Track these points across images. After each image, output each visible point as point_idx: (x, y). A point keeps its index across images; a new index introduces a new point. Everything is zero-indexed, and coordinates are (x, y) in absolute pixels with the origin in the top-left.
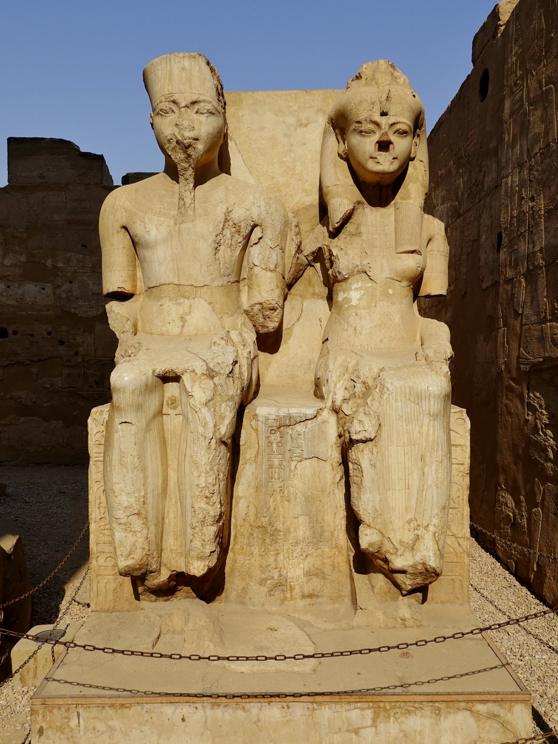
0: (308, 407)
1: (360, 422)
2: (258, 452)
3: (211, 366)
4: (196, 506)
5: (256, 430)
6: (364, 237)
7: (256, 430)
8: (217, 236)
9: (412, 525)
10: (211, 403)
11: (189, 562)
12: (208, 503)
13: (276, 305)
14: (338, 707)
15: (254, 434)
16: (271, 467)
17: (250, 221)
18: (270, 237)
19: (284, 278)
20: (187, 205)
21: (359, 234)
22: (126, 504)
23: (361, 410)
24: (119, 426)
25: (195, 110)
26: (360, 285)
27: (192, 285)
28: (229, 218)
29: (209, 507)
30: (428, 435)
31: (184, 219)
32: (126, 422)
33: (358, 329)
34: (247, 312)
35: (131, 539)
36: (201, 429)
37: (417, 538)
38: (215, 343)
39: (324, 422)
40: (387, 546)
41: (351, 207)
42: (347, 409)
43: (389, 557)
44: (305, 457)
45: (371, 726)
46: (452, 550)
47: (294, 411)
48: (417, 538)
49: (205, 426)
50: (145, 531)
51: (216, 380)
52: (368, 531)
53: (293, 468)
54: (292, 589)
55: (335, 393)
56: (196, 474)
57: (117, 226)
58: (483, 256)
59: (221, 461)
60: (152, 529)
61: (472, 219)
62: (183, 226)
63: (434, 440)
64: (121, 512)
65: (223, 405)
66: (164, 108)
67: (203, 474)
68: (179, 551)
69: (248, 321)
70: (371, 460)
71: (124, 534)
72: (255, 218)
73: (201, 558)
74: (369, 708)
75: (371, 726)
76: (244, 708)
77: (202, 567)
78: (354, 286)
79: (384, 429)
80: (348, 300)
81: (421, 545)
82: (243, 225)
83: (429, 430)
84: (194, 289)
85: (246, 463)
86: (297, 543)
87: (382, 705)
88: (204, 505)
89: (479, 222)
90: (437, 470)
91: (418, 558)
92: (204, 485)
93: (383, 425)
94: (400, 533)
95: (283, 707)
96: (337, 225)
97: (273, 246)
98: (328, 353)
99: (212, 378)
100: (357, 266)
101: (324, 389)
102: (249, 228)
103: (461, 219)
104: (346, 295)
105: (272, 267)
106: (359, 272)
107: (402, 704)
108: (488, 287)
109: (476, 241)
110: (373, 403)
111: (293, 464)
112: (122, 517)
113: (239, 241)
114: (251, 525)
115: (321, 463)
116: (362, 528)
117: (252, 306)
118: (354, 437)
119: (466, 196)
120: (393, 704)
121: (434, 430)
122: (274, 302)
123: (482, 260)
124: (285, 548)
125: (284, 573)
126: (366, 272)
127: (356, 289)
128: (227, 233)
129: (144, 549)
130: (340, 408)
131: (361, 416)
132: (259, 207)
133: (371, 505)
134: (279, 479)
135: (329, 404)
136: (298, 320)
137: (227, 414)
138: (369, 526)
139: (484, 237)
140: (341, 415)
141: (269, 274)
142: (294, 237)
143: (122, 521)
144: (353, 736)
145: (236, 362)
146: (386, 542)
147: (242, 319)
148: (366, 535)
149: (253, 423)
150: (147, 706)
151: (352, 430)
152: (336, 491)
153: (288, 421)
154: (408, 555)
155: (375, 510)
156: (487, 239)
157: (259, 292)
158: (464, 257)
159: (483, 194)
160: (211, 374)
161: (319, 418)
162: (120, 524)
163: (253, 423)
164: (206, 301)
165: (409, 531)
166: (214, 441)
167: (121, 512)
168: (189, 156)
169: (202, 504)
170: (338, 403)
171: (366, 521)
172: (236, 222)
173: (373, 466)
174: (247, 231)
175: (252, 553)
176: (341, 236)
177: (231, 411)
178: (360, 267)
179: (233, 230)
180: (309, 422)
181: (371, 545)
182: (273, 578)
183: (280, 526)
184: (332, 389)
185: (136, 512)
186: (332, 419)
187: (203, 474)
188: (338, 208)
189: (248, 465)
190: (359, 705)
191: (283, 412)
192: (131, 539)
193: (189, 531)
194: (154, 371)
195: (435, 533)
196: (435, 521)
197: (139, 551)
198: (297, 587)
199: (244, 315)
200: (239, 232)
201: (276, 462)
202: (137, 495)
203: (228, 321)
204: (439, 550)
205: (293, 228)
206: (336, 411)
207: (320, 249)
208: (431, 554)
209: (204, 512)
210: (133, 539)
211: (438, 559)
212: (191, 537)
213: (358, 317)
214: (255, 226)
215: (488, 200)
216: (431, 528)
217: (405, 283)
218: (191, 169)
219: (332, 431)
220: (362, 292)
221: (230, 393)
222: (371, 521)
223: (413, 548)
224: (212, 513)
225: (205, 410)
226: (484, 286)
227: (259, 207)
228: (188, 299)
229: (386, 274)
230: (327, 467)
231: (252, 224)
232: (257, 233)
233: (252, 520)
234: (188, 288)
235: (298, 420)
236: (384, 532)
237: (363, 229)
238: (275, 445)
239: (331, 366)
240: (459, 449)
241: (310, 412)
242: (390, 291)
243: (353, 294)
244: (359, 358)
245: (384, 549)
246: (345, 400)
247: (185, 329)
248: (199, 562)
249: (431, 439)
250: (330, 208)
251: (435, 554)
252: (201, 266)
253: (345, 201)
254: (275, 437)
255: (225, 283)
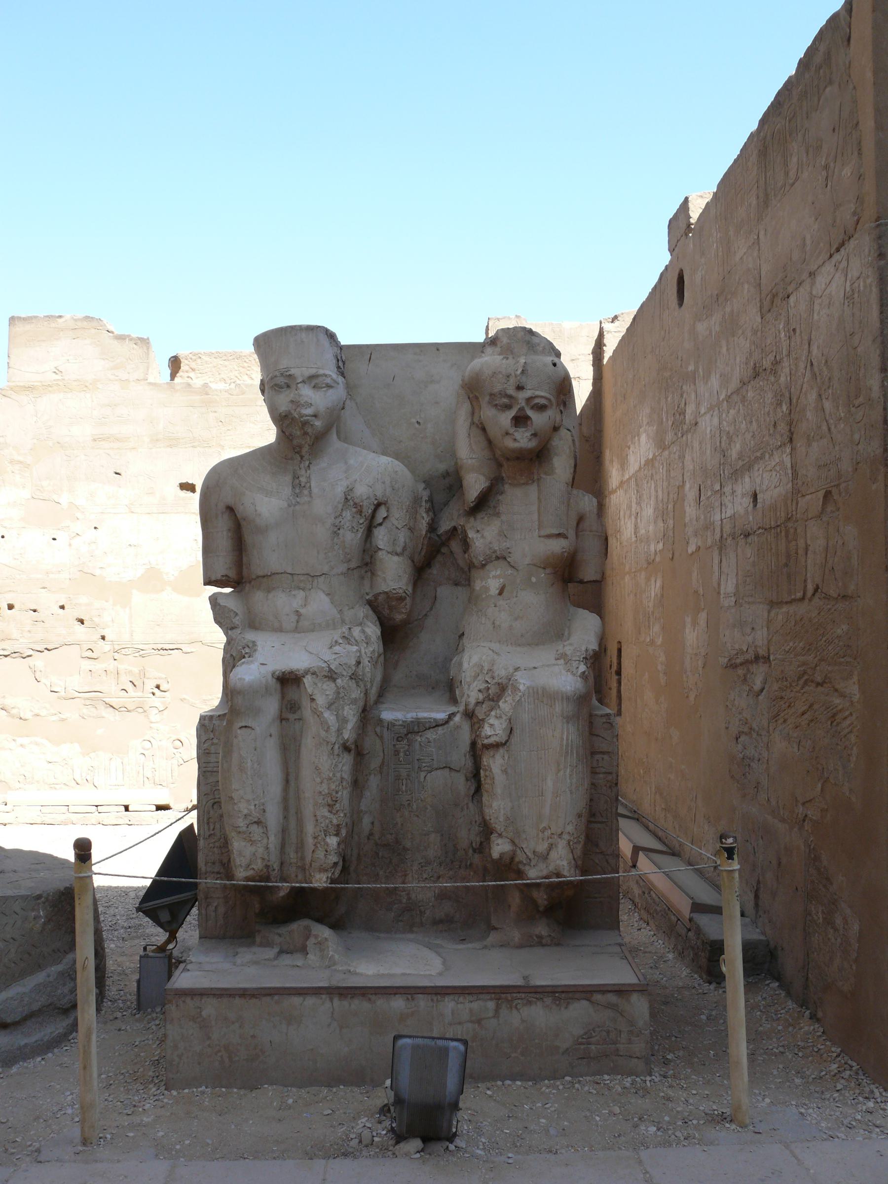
0: (438, 712)
1: (491, 725)
2: (383, 762)
3: (333, 667)
4: (318, 813)
5: (381, 738)
6: (504, 518)
7: (381, 738)
8: (336, 518)
9: (546, 833)
10: (333, 707)
11: (310, 875)
12: (329, 811)
13: (404, 595)
14: (461, 999)
15: (378, 741)
16: (398, 778)
17: (373, 500)
18: (398, 516)
19: (413, 561)
20: (303, 485)
21: (498, 515)
22: (246, 812)
23: (493, 713)
24: (239, 731)
25: (313, 384)
26: (498, 573)
27: (307, 574)
28: (349, 497)
29: (332, 816)
30: (562, 739)
31: (298, 500)
32: (246, 727)
33: (497, 623)
34: (370, 603)
35: (249, 850)
36: (323, 734)
37: (551, 847)
38: (336, 642)
39: (458, 727)
40: (520, 857)
41: (487, 484)
42: (480, 713)
43: (521, 866)
44: (435, 766)
45: (494, 1017)
46: (599, 869)
47: (423, 715)
48: (551, 847)
49: (327, 730)
50: (265, 841)
51: (339, 681)
52: (500, 841)
53: (422, 780)
54: (422, 913)
55: (468, 696)
56: (318, 780)
57: (221, 506)
58: (687, 509)
59: (344, 768)
60: (272, 838)
61: (676, 456)
62: (297, 507)
63: (567, 745)
64: (241, 820)
65: (346, 708)
66: (278, 382)
67: (325, 781)
68: (299, 864)
69: (371, 612)
70: (502, 766)
71: (243, 844)
72: (379, 494)
73: (322, 870)
74: (491, 999)
75: (494, 1017)
76: (370, 999)
77: (324, 879)
78: (493, 573)
79: (517, 732)
80: (487, 589)
81: (553, 855)
82: (365, 503)
83: (563, 733)
84: (310, 579)
85: (370, 774)
86: (428, 863)
87: (503, 996)
88: (327, 814)
89: (683, 463)
90: (570, 775)
91: (551, 868)
92: (326, 791)
93: (514, 729)
94: (534, 844)
95: (408, 999)
96: (472, 505)
97: (400, 527)
98: (463, 650)
99: (334, 680)
100: (495, 552)
101: (457, 693)
102: (373, 507)
103: (666, 453)
104: (484, 583)
105: (399, 550)
106: (498, 558)
107: (523, 995)
108: (692, 553)
109: (681, 487)
110: (506, 705)
111: (423, 774)
112: (242, 825)
113: (361, 522)
114: (377, 844)
115: (453, 774)
116: (493, 837)
117: (376, 596)
118: (486, 741)
119: (670, 423)
120: (515, 995)
121: (568, 733)
122: (401, 591)
123: (687, 515)
124: (415, 868)
125: (413, 896)
126: (505, 558)
127: (495, 577)
128: (347, 514)
129: (263, 859)
130: (473, 712)
131: (492, 721)
132: (384, 483)
133: (502, 812)
134: (406, 792)
135: (462, 708)
136: (431, 609)
137: (350, 717)
138: (500, 835)
139: (687, 486)
140: (475, 720)
141: (396, 558)
142: (425, 515)
143: (241, 830)
144: (477, 1025)
145: (358, 663)
146: (519, 852)
147: (363, 611)
148: (498, 845)
149: (378, 729)
150: (276, 997)
151: (483, 734)
152: (470, 804)
153: (416, 728)
154: (542, 866)
155: (507, 819)
156: (690, 488)
157: (385, 580)
158: (670, 506)
159: (685, 427)
160: (331, 676)
161: (452, 723)
162: (240, 832)
163: (378, 729)
164: (324, 591)
165: (543, 840)
166: (337, 746)
167: (241, 820)
168: (306, 433)
169: (325, 812)
170: (471, 707)
171: (498, 830)
172: (357, 501)
173: (505, 771)
174: (370, 511)
175: (378, 874)
176: (480, 516)
177: (354, 715)
178: (498, 553)
179: (354, 510)
180: (440, 728)
181: (502, 855)
182: (401, 902)
183: (408, 844)
184: (466, 692)
185: (256, 820)
186: (466, 727)
187: (325, 781)
188: (475, 484)
189: (372, 776)
190: (481, 996)
191: (410, 716)
192: (249, 850)
193: (310, 841)
194: (273, 674)
195: (569, 842)
196: (570, 828)
197: (259, 861)
198: (428, 912)
199: (367, 607)
200: (360, 512)
201: (404, 773)
202: (257, 802)
203: (349, 614)
204: (574, 859)
205: (424, 504)
206: (469, 715)
207: (455, 529)
208: (565, 863)
209: (327, 821)
210: (253, 849)
211: (573, 869)
212: (313, 847)
213: (497, 609)
214: (378, 505)
215: (689, 436)
216: (566, 837)
217: (548, 571)
218: (307, 446)
219: (465, 737)
220: (501, 580)
221: (353, 696)
222: (502, 830)
223: (546, 858)
224: (335, 822)
225: (327, 714)
226: (690, 551)
227: (384, 483)
228: (303, 590)
229: (527, 561)
230: (462, 779)
231: (376, 502)
232: (382, 513)
233: (377, 837)
234: (302, 578)
235: (427, 726)
236: (517, 841)
237: (502, 508)
238: (402, 754)
239: (465, 665)
240: (606, 757)
241: (441, 716)
242: (534, 580)
243: (491, 581)
244: (496, 657)
245: (517, 860)
246: (478, 703)
247: (300, 624)
248: (322, 875)
249: (565, 742)
250: (465, 483)
251: (569, 863)
252: (318, 553)
253: (482, 478)
254: (403, 745)
255: (345, 570)
